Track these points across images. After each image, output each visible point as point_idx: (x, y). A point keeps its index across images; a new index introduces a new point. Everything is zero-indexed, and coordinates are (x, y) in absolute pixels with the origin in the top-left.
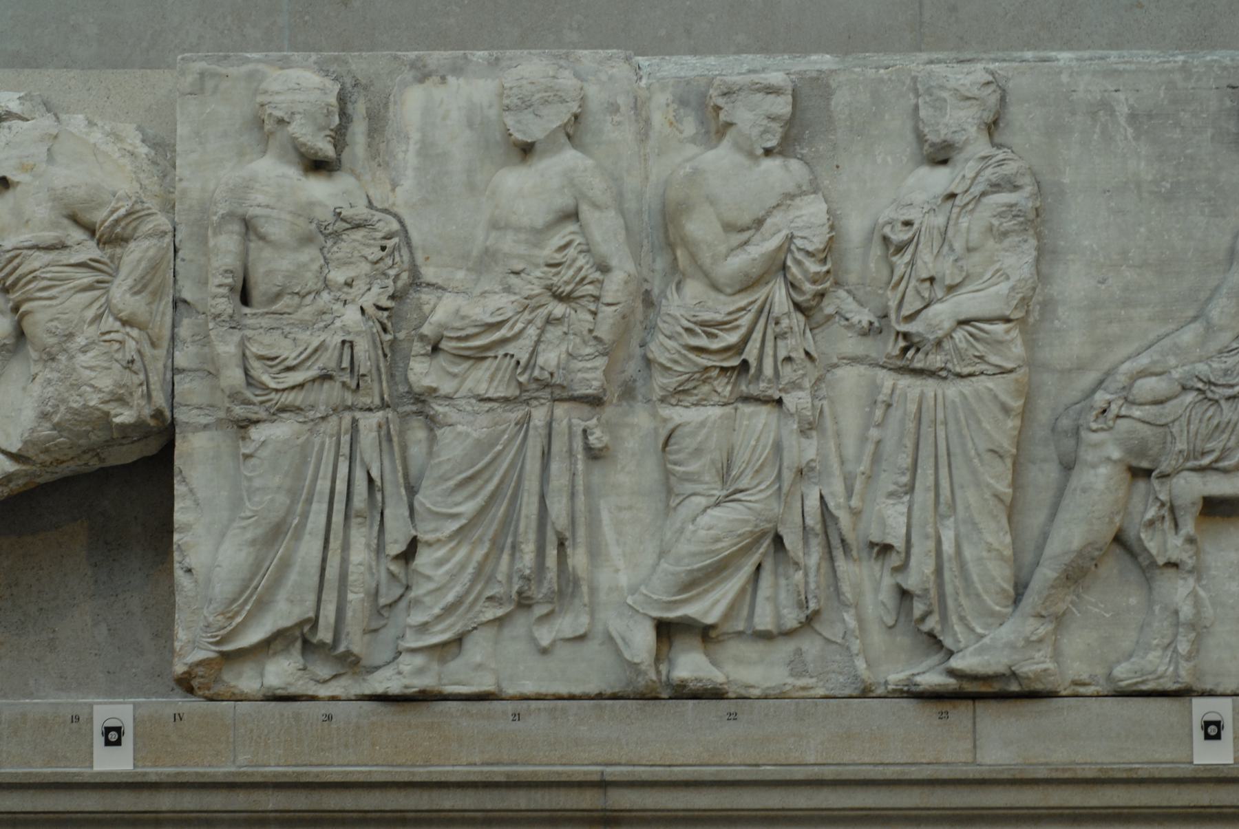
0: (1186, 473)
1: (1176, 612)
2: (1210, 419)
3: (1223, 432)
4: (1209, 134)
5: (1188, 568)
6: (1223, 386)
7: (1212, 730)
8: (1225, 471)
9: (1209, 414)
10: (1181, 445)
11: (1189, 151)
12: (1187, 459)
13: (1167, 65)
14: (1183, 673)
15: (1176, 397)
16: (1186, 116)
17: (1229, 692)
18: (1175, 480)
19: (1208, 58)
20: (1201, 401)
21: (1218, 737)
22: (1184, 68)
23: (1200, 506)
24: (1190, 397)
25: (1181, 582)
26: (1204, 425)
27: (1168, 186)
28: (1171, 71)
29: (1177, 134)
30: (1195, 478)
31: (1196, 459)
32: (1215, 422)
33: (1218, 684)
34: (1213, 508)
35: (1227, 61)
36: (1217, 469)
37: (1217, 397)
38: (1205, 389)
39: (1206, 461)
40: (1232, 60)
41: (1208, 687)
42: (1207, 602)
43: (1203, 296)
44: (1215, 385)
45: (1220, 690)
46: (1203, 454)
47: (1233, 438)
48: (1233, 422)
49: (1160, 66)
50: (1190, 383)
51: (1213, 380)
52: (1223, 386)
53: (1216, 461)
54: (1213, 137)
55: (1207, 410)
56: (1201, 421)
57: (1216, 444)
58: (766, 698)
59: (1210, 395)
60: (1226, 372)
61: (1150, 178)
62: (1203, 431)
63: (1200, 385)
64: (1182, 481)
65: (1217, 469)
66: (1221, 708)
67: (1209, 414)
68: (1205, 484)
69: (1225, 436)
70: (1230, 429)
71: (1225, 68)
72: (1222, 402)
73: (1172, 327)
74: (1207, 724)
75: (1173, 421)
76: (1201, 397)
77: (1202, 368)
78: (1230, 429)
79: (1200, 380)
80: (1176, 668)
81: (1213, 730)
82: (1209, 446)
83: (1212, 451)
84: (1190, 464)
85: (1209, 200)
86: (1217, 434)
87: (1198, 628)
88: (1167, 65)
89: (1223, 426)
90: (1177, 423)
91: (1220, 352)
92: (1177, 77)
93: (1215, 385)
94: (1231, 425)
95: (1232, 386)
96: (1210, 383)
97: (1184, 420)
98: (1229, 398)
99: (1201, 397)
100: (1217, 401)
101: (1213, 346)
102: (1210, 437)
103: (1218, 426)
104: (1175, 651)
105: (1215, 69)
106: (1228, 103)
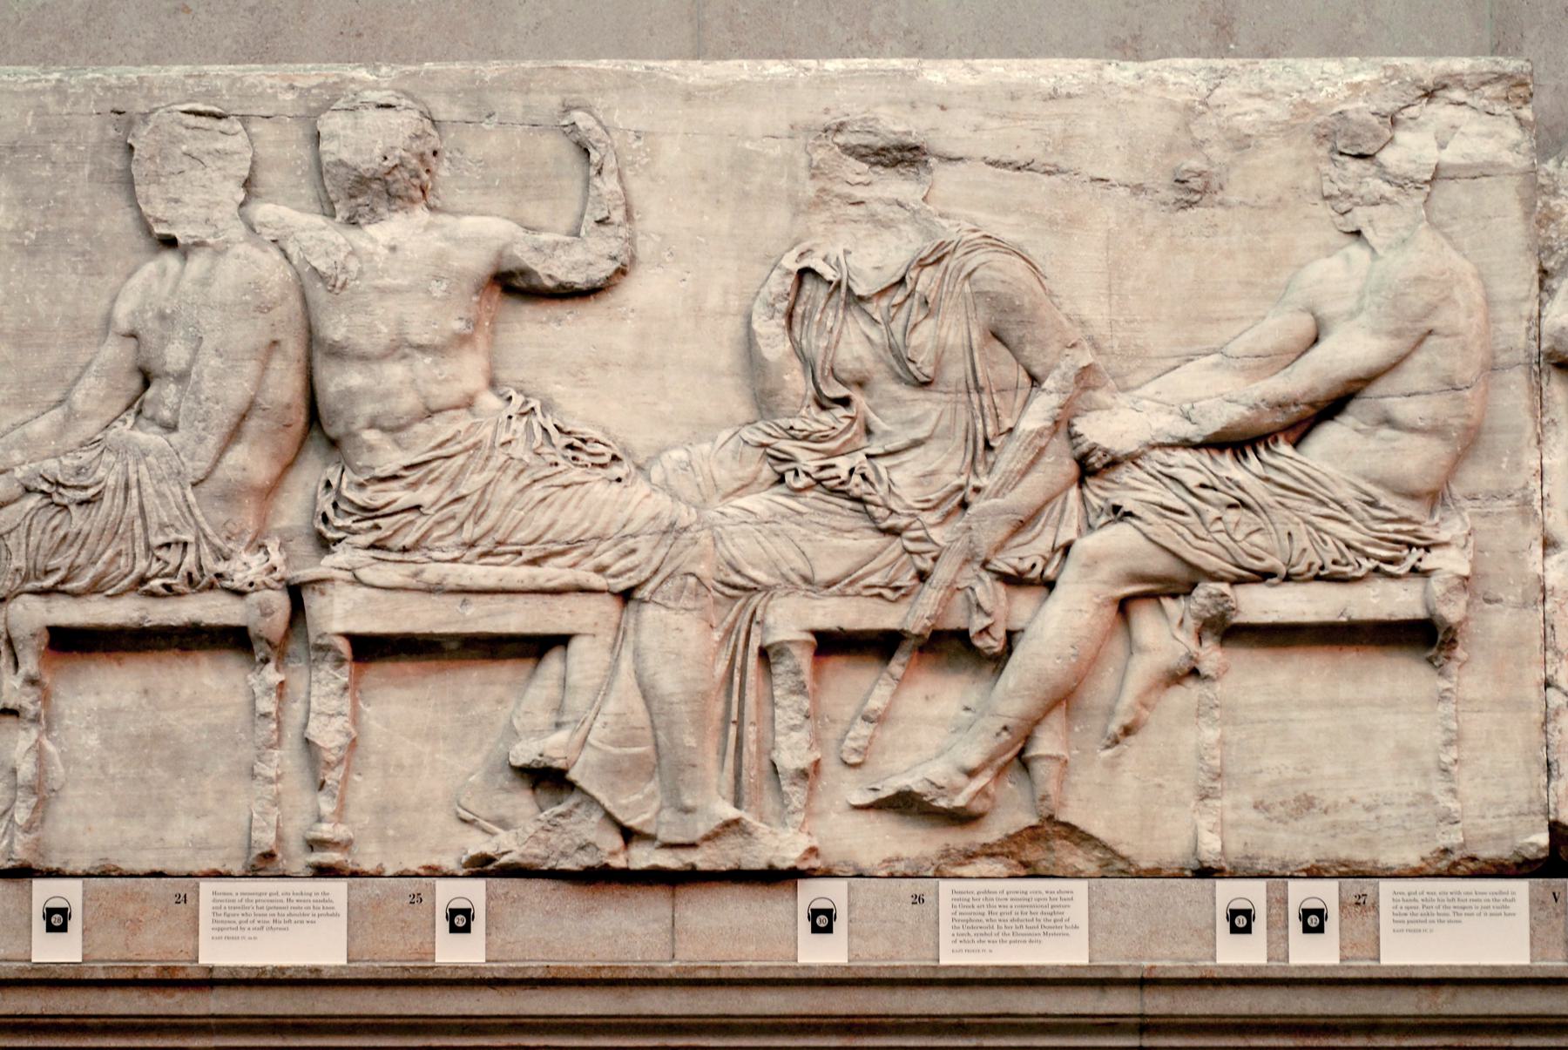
0: (25, 597)
1: (14, 772)
2: (55, 529)
3: (71, 545)
4: (87, 172)
5: (30, 715)
6: (74, 487)
7: (57, 920)
8: (75, 595)
9: (55, 522)
10: (18, 562)
11: (60, 193)
12: (26, 579)
13: (37, 85)
14: (17, 847)
15: (16, 501)
16: (57, 149)
17: (80, 872)
18: (11, 606)
19: (90, 76)
20: (47, 506)
21: (1320, 929)
22: (59, 89)
23: (45, 638)
24: (33, 501)
25: (22, 733)
26: (47, 536)
27: (33, 236)
28: (43, 92)
29: (46, 172)
30: (36, 603)
31: (37, 579)
32: (61, 533)
33: (66, 863)
34: (69, 643)
35: (113, 81)
36: (64, 592)
37: (65, 501)
38: (52, 493)
39: (49, 582)
40: (119, 78)
41: (54, 866)
42: (57, 760)
43: (70, 375)
44: (65, 486)
45: (69, 869)
46: (47, 573)
47: (83, 553)
48: (85, 532)
49: (28, 86)
50: (33, 485)
51: (61, 480)
52: (74, 487)
53: (63, 581)
54: (91, 175)
55: (53, 517)
56: (43, 532)
57: (62, 561)
58: (104, 875)
59: (56, 499)
60: (79, 471)
61: (10, 226)
62: (46, 545)
63: (45, 487)
64: (20, 607)
65: (64, 592)
66: (69, 893)
67: (55, 522)
68: (49, 611)
69: (73, 551)
70: (79, 542)
71: (109, 88)
72: (73, 508)
73: (30, 413)
74: (50, 913)
75: (9, 533)
76: (46, 501)
77: (51, 466)
78: (79, 542)
79: (46, 480)
80: (11, 843)
81: (57, 919)
82: (53, 563)
83: (58, 569)
84: (29, 586)
85: (83, 254)
86: (63, 548)
87: (42, 793)
88: (37, 85)
89: (70, 538)
90: (13, 534)
91: (82, 445)
92: (49, 100)
93: (65, 486)
94: (81, 537)
95: (85, 488)
96: (58, 484)
97: (22, 530)
98: (81, 503)
99: (46, 501)
100: (66, 507)
101: (73, 438)
102: (54, 552)
103: (65, 537)
104: (12, 820)
105: (97, 89)
106: (112, 133)
